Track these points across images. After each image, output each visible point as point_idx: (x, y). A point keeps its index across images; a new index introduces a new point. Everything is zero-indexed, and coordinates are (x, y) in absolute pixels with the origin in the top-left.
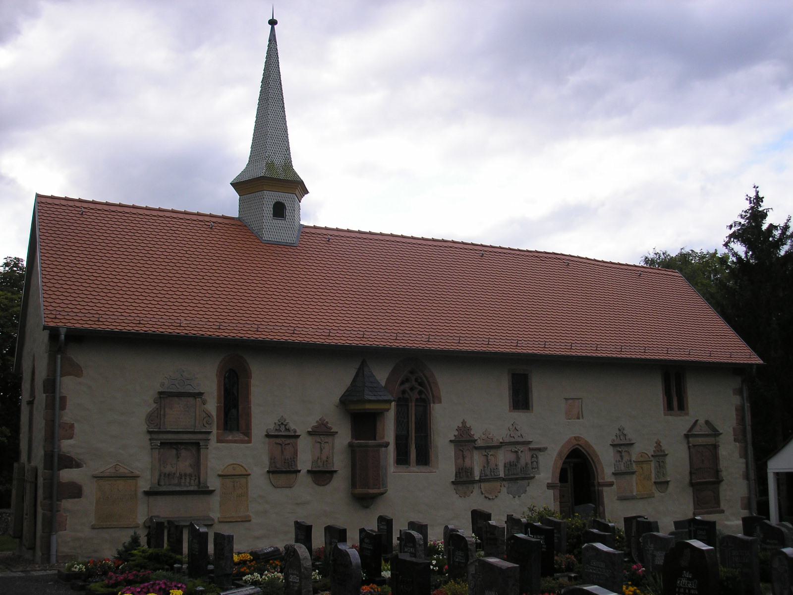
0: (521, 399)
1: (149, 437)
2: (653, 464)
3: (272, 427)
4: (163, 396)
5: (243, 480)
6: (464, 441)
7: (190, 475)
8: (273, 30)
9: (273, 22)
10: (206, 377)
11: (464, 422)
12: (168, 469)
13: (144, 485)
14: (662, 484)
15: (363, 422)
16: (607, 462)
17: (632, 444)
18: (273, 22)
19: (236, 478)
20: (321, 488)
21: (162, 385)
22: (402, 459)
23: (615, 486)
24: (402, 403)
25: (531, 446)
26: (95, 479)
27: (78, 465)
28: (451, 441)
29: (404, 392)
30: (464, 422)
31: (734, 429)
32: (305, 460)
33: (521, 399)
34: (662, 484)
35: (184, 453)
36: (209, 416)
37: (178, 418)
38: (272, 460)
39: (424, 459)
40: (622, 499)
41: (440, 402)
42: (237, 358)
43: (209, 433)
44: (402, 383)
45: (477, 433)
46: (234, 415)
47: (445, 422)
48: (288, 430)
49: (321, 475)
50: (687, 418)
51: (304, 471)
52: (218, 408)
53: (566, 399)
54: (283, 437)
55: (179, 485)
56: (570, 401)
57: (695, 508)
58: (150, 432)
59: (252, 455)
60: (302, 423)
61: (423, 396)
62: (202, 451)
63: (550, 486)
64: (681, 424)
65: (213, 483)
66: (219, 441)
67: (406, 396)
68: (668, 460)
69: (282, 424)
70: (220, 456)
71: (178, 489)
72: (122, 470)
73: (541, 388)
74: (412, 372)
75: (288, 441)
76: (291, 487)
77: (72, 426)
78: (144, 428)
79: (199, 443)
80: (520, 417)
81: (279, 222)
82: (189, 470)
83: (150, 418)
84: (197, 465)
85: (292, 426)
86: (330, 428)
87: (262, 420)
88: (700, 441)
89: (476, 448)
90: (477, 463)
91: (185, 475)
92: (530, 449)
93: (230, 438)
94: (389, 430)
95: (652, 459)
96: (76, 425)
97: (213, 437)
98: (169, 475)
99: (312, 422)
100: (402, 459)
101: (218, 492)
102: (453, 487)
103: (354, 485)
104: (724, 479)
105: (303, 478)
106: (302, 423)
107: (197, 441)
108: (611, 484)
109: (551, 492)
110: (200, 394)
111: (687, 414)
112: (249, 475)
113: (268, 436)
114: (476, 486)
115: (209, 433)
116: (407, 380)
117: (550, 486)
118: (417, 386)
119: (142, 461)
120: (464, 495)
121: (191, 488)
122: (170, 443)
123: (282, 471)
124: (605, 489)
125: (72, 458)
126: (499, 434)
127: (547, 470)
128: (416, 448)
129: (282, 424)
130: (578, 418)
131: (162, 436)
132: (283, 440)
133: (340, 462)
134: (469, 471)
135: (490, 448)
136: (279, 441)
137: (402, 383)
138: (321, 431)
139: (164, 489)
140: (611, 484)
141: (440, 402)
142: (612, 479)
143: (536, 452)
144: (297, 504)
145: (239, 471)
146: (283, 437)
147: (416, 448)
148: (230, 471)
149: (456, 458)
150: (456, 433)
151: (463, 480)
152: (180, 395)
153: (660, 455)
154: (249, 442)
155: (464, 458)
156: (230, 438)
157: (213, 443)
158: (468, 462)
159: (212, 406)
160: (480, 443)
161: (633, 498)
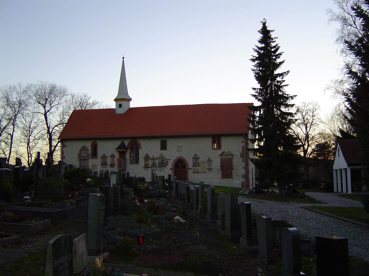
0: (164, 147)
2: (207, 164)
3: (102, 155)
6: (147, 158)
8: (123, 60)
9: (123, 58)
10: (88, 145)
11: (147, 153)
14: (210, 170)
15: (122, 154)
16: (190, 162)
17: (200, 158)
18: (123, 58)
22: (132, 163)
23: (192, 169)
24: (132, 149)
25: (166, 159)
30: (147, 153)
31: (241, 153)
32: (109, 163)
33: (164, 147)
34: (210, 170)
37: (84, 154)
38: (102, 162)
39: (137, 162)
40: (194, 173)
43: (89, 157)
45: (151, 156)
46: (94, 154)
47: (142, 154)
48: (105, 156)
50: (221, 150)
52: (92, 153)
53: (178, 147)
54: (104, 157)
56: (179, 147)
57: (222, 177)
60: (108, 155)
63: (171, 169)
64: (220, 152)
68: (213, 163)
69: (104, 155)
73: (170, 143)
74: (135, 142)
77: (65, 157)
80: (164, 152)
81: (120, 108)
83: (78, 154)
87: (100, 154)
88: (225, 157)
89: (150, 159)
90: (150, 163)
92: (166, 160)
93: (93, 158)
94: (128, 156)
95: (207, 162)
97: (90, 158)
104: (234, 168)
106: (108, 155)
108: (191, 169)
109: (171, 170)
111: (221, 149)
116: (134, 144)
117: (171, 169)
124: (189, 170)
126: (157, 156)
127: (170, 165)
129: (104, 155)
130: (182, 151)
133: (116, 163)
134: (149, 165)
135: (154, 159)
137: (133, 145)
138: (113, 156)
140: (191, 169)
142: (192, 168)
143: (168, 160)
151: (146, 167)
153: (210, 160)
159: (90, 152)
160: (151, 158)
161: (198, 172)
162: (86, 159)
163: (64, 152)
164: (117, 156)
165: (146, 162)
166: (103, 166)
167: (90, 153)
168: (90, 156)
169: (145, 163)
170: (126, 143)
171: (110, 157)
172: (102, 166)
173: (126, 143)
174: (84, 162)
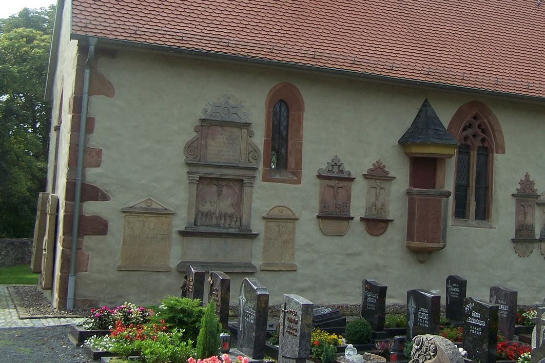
1: (186, 170)
3: (324, 167)
4: (207, 125)
5: (290, 225)
7: (231, 216)
10: (253, 103)
11: (527, 176)
12: (207, 207)
13: (180, 222)
15: (424, 169)
19: (282, 220)
20: (375, 238)
21: (205, 111)
22: (461, 212)
24: (464, 150)
26: (124, 215)
27: (105, 198)
28: (513, 195)
29: (466, 138)
30: (527, 176)
32: (358, 208)
35: (225, 190)
36: (256, 150)
37: (220, 149)
38: (323, 203)
39: (483, 213)
41: (504, 152)
42: (290, 85)
43: (255, 169)
44: (465, 129)
46: (282, 150)
48: (342, 171)
49: (376, 224)
51: (357, 219)
52: (266, 143)
54: (336, 178)
55: (218, 226)
58: (188, 164)
59: (302, 197)
61: (486, 145)
62: (246, 190)
65: (257, 226)
66: (265, 179)
67: (469, 143)
69: (336, 164)
70: (264, 197)
71: (216, 230)
72: (154, 206)
75: (341, 184)
76: (342, 236)
77: (99, 153)
78: (182, 159)
79: (242, 180)
82: (230, 210)
83: (190, 148)
84: (238, 205)
85: (347, 168)
86: (387, 173)
91: (225, 215)
94: (448, 181)
96: (103, 151)
97: (259, 175)
98: (208, 215)
99: (368, 164)
100: (461, 212)
101: (262, 236)
102: (512, 245)
103: (410, 237)
105: (357, 227)
106: (357, 166)
107: (241, 178)
110: (247, 125)
112: (297, 219)
113: (320, 177)
114: (536, 245)
115: (255, 169)
116: (470, 126)
118: (479, 132)
119: (177, 197)
120: (522, 255)
121: (232, 231)
122: (207, 177)
123: (333, 216)
125: (98, 189)
128: (475, 201)
129: (336, 164)
131: (201, 170)
132: (336, 182)
133: (396, 210)
134: (531, 228)
136: (332, 183)
138: (378, 175)
139: (202, 229)
141: (504, 152)
144: (349, 255)
145: (286, 213)
146: (336, 178)
147: (475, 201)
148: (276, 213)
149: (517, 214)
150: (519, 187)
152: (223, 124)
154: (299, 182)
155: (525, 215)
156: (278, 177)
157: (259, 181)
158: (529, 220)
159: (259, 139)
162: (233, 180)
163: (90, 122)
164: (400, 173)
165: (521, 217)
166: (333, 225)
167: (261, 148)
168: (261, 167)
169: (517, 220)
170: (445, 115)
171: (365, 177)
172: (326, 222)
173: (445, 115)
174: (220, 194)
